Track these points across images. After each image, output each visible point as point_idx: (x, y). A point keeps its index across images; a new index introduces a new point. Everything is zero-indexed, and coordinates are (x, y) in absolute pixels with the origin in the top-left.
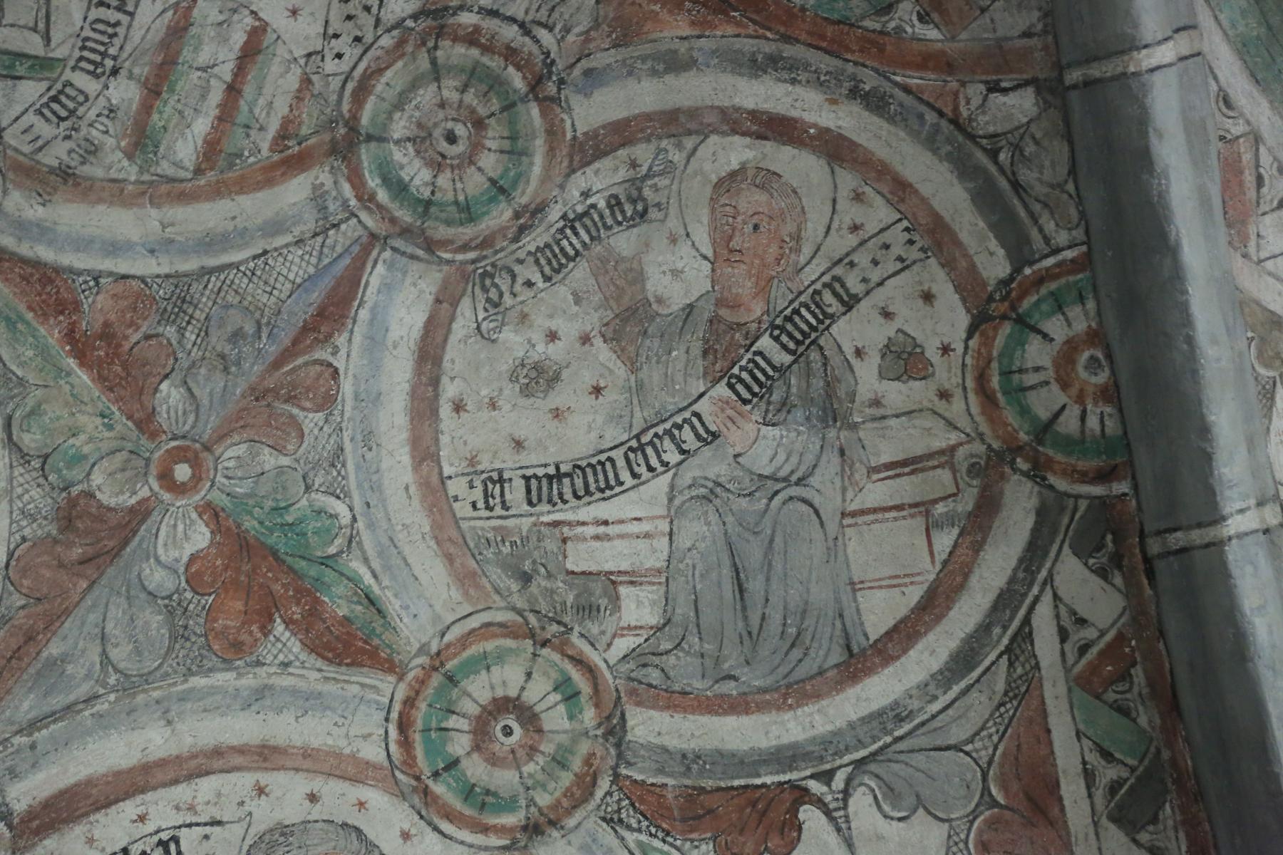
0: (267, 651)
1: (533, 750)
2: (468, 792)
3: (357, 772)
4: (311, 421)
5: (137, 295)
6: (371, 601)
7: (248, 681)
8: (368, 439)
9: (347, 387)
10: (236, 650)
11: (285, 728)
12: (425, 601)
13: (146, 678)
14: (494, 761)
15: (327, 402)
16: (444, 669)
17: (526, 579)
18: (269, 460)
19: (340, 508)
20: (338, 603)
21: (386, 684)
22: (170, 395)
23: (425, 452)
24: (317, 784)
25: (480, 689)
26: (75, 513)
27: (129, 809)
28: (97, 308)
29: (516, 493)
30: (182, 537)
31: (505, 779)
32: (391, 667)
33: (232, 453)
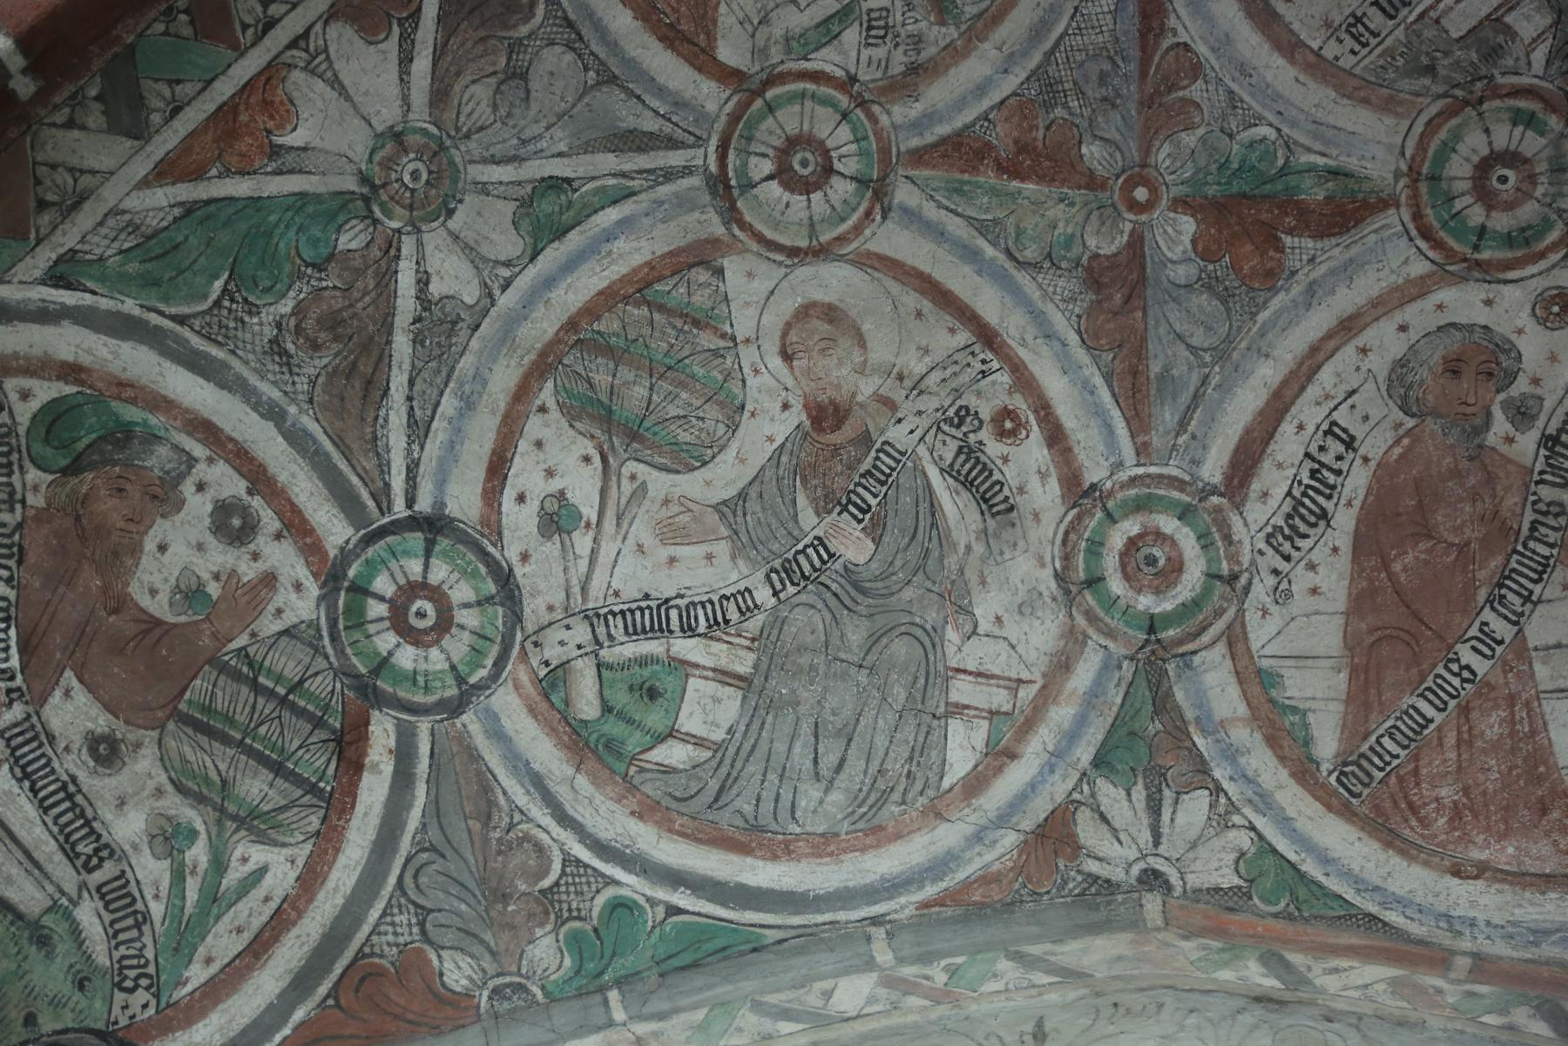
0: (1292, 261)
1: (1532, 179)
2: (1509, 240)
3: (1418, 289)
4: (1196, 91)
5: (1018, 107)
6: (1334, 173)
7: (1296, 290)
8: (1244, 70)
9: (1202, 49)
10: (1272, 277)
11: (1346, 299)
12: (1372, 143)
13: (1228, 340)
14: (1510, 206)
15: (1196, 70)
16: (1423, 175)
17: (1431, 70)
18: (1189, 139)
19: (1264, 131)
20: (1314, 193)
21: (1390, 217)
22: (1092, 152)
23: (1289, 46)
24: (1399, 317)
25: (1459, 169)
26: (1096, 275)
27: (1287, 427)
28: (1001, 136)
29: (1376, 19)
30: (1176, 234)
31: (1528, 212)
32: (1387, 203)
33: (1162, 155)
